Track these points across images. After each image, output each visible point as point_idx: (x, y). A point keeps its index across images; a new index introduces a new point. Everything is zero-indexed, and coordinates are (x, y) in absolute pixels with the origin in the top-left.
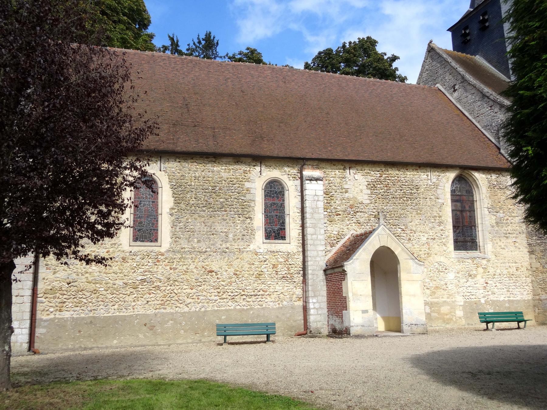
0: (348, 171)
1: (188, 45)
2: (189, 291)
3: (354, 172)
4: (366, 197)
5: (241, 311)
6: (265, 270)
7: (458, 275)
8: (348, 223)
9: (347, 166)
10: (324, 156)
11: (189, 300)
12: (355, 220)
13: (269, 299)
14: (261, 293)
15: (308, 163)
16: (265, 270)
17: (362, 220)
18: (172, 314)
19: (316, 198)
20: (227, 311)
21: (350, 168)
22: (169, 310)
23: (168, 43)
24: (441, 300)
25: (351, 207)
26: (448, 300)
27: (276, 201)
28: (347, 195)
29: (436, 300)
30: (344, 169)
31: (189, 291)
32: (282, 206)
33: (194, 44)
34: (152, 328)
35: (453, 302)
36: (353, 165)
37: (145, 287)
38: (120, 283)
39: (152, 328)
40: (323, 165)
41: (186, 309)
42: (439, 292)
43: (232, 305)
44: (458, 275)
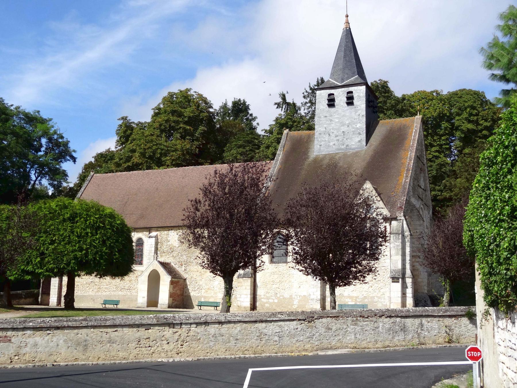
0: (170, 231)
1: (303, 93)
2: (106, 286)
3: (173, 231)
4: (177, 243)
5: (124, 295)
6: (133, 278)
7: (220, 282)
8: (168, 256)
9: (170, 228)
10: (160, 225)
11: (106, 290)
12: (171, 255)
13: (134, 291)
14: (131, 288)
15: (153, 229)
16: (133, 278)
17: (174, 255)
18: (100, 295)
19: (151, 246)
20: (118, 295)
21: (171, 230)
22: (100, 294)
23: (280, 100)
24: (210, 295)
25: (171, 249)
26: (214, 295)
27: (141, 248)
28: (169, 243)
29: (207, 295)
30: (169, 230)
31: (106, 286)
32: (142, 250)
33: (306, 92)
34: (94, 300)
35: (216, 297)
36: (172, 228)
37: (93, 284)
38: (85, 282)
39: (94, 300)
40: (159, 229)
41: (105, 294)
42: (209, 291)
43: (120, 293)
44: (220, 282)
